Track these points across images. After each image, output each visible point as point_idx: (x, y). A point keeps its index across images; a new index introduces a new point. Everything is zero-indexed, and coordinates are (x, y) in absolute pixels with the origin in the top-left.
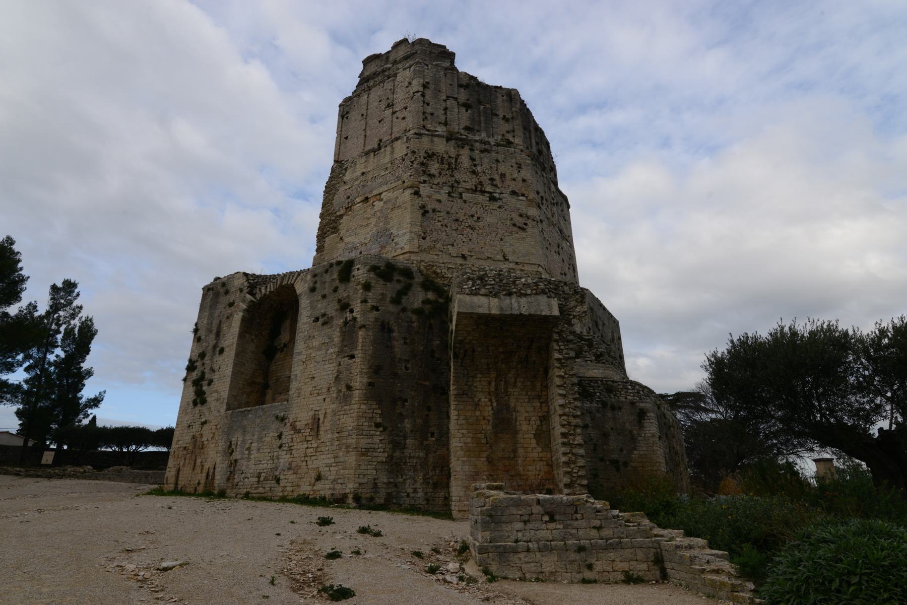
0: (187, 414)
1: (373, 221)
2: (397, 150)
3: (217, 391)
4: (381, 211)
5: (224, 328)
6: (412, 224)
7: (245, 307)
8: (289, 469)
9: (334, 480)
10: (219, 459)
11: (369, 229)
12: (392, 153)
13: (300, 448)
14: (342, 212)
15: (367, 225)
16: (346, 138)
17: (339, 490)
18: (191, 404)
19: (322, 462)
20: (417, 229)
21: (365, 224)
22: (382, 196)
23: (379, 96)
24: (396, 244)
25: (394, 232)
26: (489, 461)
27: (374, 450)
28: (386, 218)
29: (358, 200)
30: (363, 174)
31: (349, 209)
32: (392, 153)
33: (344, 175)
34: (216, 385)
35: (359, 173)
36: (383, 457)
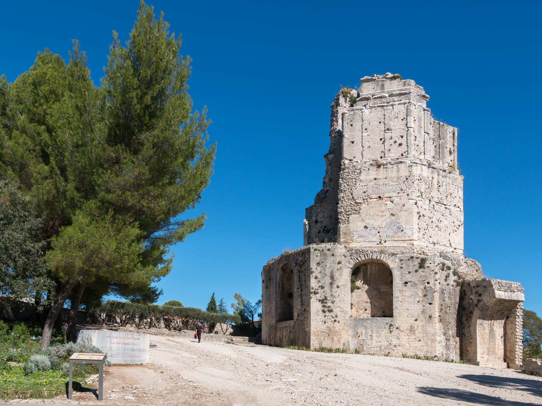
0: (318, 315)
3: (339, 307)
5: (337, 275)
7: (351, 266)
8: (399, 345)
9: (427, 352)
10: (350, 339)
11: (384, 218)
12: (398, 171)
15: (382, 216)
16: (353, 142)
21: (380, 214)
23: (378, 118)
24: (405, 233)
25: (404, 226)
26: (488, 349)
27: (442, 342)
30: (375, 179)
32: (398, 171)
34: (338, 303)
35: (372, 177)
36: (444, 344)
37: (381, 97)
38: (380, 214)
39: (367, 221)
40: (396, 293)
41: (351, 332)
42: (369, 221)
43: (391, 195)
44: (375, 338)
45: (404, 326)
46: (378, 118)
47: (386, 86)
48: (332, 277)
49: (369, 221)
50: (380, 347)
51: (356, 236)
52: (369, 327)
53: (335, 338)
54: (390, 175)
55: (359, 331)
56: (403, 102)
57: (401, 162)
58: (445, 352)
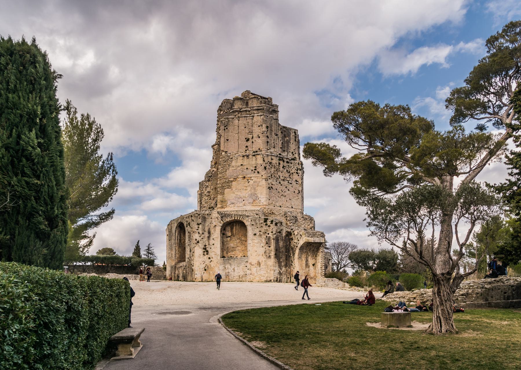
0: (200, 258)
1: (249, 188)
2: (258, 160)
4: (252, 185)
5: (212, 231)
6: (266, 194)
7: (221, 225)
11: (247, 191)
12: (256, 160)
13: (254, 270)
14: (232, 180)
15: (246, 190)
16: (228, 140)
17: (269, 279)
18: (202, 255)
19: (262, 272)
20: (268, 196)
22: (252, 178)
23: (244, 124)
24: (260, 201)
25: (259, 196)
28: (255, 189)
29: (241, 177)
30: (242, 165)
31: (235, 179)
32: (256, 160)
33: (232, 161)
35: (240, 164)
37: (246, 111)
38: (245, 188)
39: (236, 193)
40: (249, 241)
41: (221, 267)
42: (238, 193)
43: (251, 176)
44: (236, 270)
45: (254, 262)
46: (244, 124)
47: (249, 104)
48: (209, 233)
49: (238, 193)
50: (239, 276)
51: (229, 203)
52: (232, 263)
53: (211, 272)
54: (251, 162)
55: (226, 267)
56: (259, 114)
57: (258, 155)
58: (279, 276)
